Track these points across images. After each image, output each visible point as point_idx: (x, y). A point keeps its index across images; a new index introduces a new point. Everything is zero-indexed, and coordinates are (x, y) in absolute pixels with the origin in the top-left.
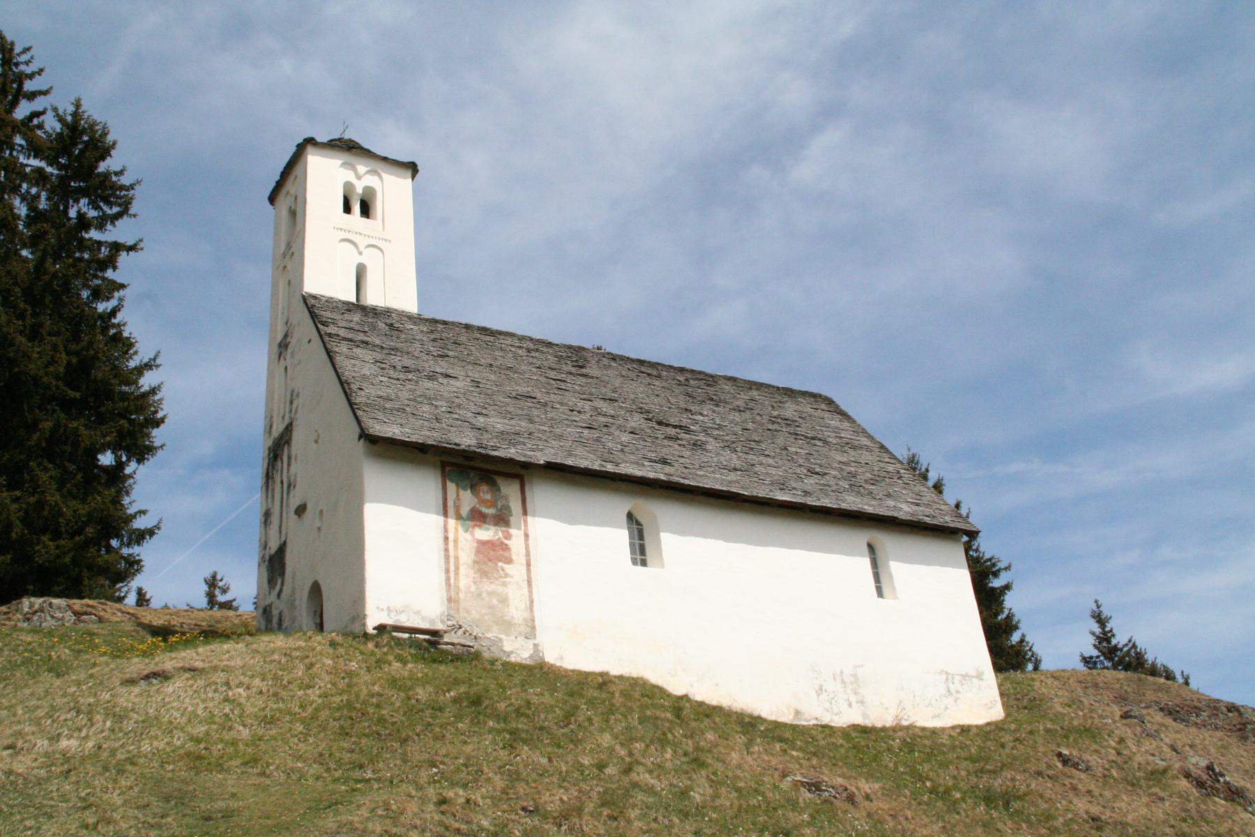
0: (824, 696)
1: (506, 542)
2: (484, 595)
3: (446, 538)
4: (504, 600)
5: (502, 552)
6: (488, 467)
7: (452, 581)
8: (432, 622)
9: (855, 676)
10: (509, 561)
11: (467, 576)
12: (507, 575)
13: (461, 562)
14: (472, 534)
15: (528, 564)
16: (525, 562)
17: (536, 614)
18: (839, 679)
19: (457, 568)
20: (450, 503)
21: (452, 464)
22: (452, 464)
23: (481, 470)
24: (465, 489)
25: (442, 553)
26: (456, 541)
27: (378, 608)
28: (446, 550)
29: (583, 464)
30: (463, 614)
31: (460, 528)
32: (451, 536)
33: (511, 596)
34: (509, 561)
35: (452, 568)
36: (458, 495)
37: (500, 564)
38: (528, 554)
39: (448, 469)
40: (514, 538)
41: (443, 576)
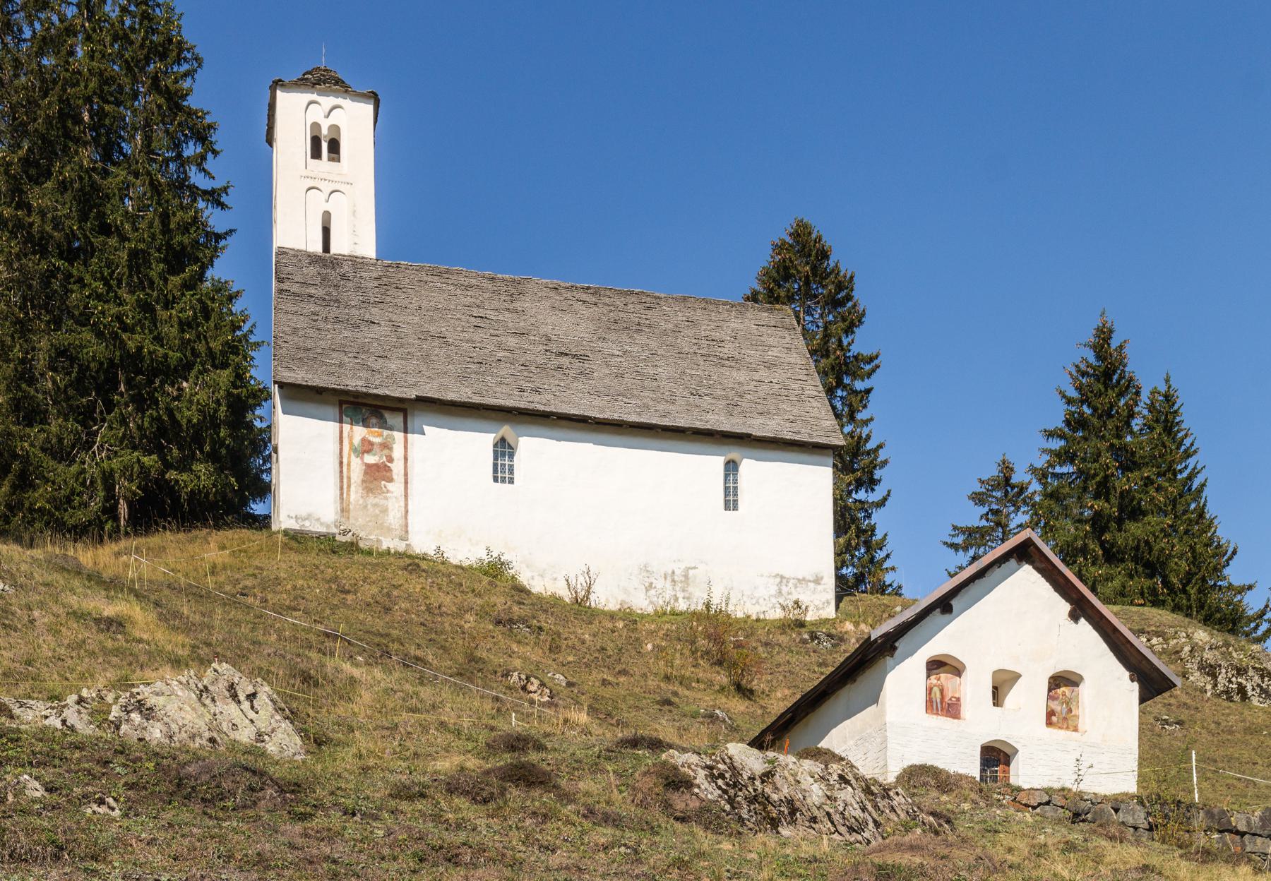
0: (652, 592)
1: (389, 464)
2: (369, 506)
3: (341, 463)
4: (385, 511)
5: (385, 473)
6: (379, 403)
7: (345, 495)
8: (328, 526)
9: (686, 576)
10: (391, 480)
11: (357, 492)
12: (388, 491)
13: (352, 481)
14: (362, 459)
15: (406, 482)
16: (403, 480)
17: (409, 521)
18: (669, 579)
19: (349, 486)
20: (345, 434)
21: (347, 402)
22: (347, 402)
23: (370, 406)
24: (357, 423)
25: (338, 475)
26: (349, 465)
27: (289, 516)
28: (341, 472)
29: (451, 396)
30: (352, 521)
31: (352, 455)
32: (345, 461)
33: (390, 507)
34: (391, 480)
35: (345, 486)
36: (351, 428)
37: (383, 482)
38: (406, 474)
39: (344, 406)
40: (395, 461)
41: (338, 492)
